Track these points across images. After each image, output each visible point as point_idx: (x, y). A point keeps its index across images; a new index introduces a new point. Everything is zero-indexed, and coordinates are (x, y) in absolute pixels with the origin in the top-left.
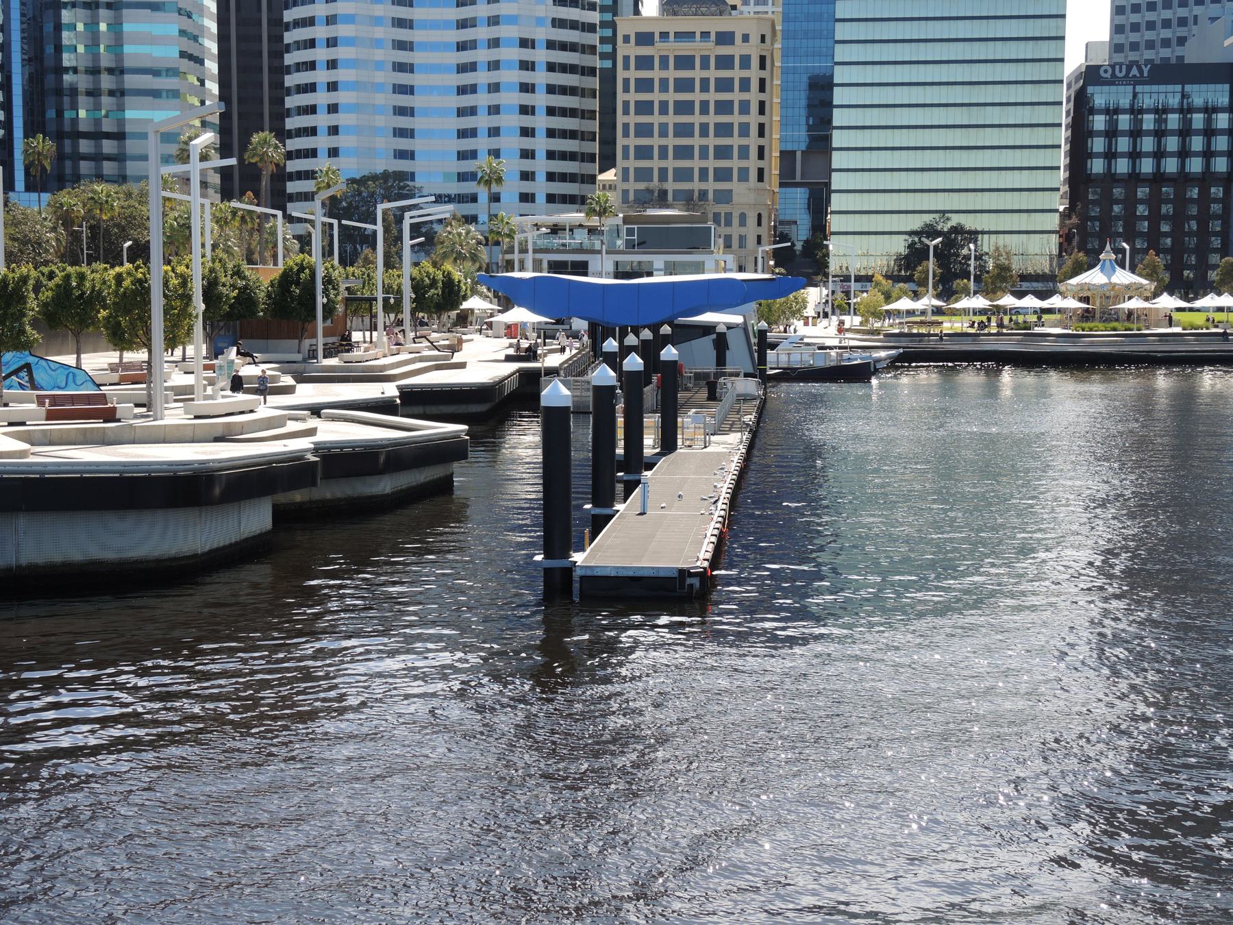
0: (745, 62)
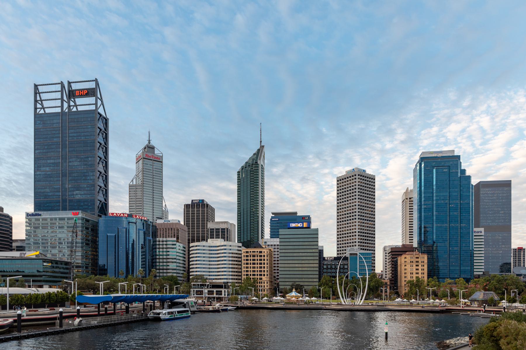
0: (264, 256)
